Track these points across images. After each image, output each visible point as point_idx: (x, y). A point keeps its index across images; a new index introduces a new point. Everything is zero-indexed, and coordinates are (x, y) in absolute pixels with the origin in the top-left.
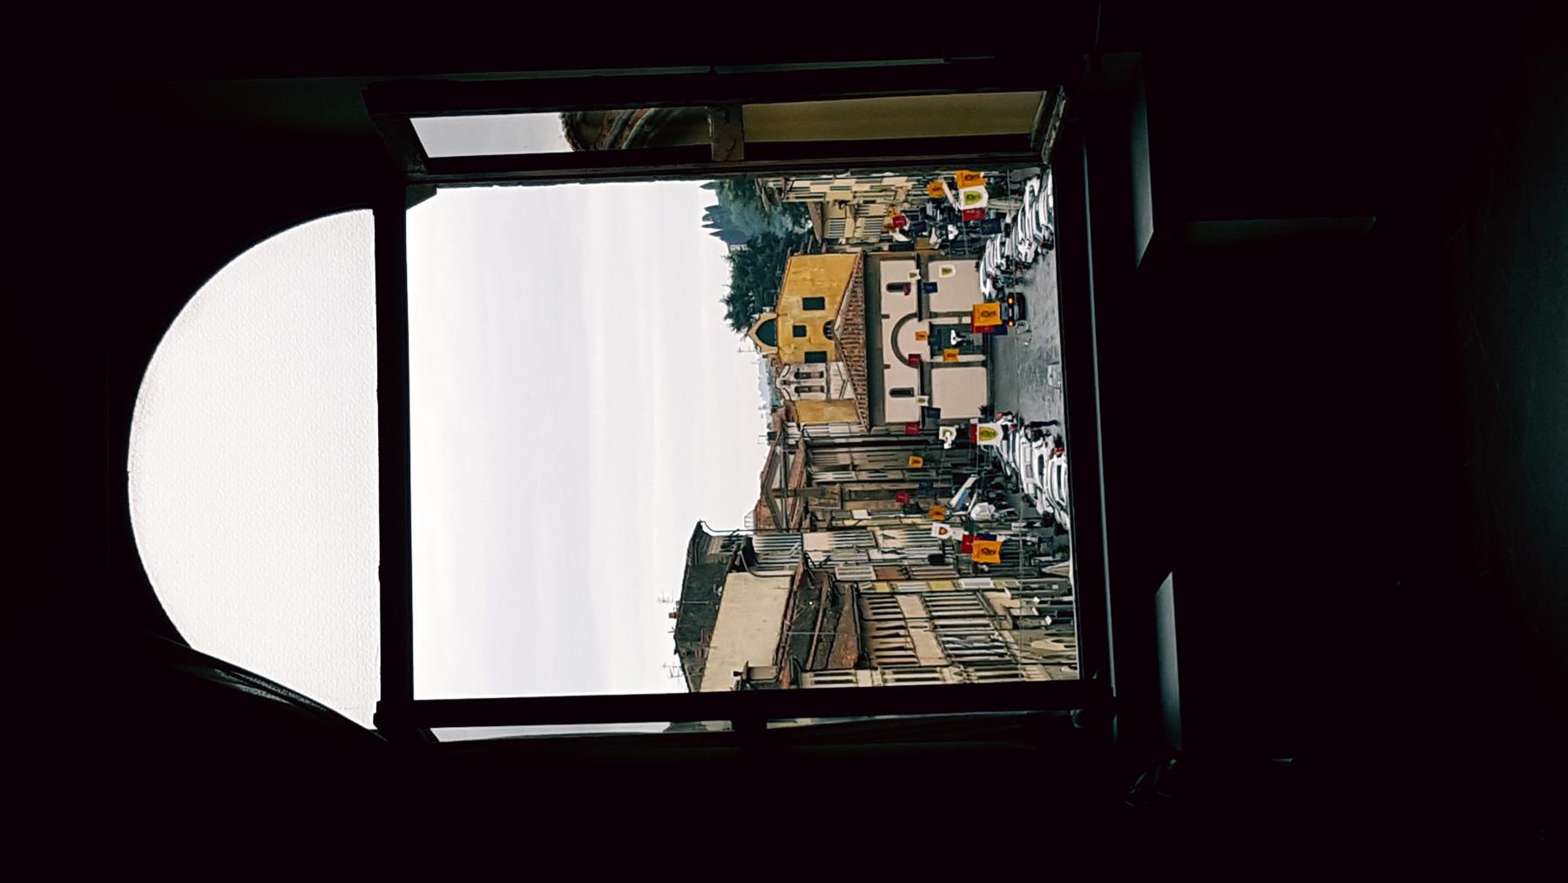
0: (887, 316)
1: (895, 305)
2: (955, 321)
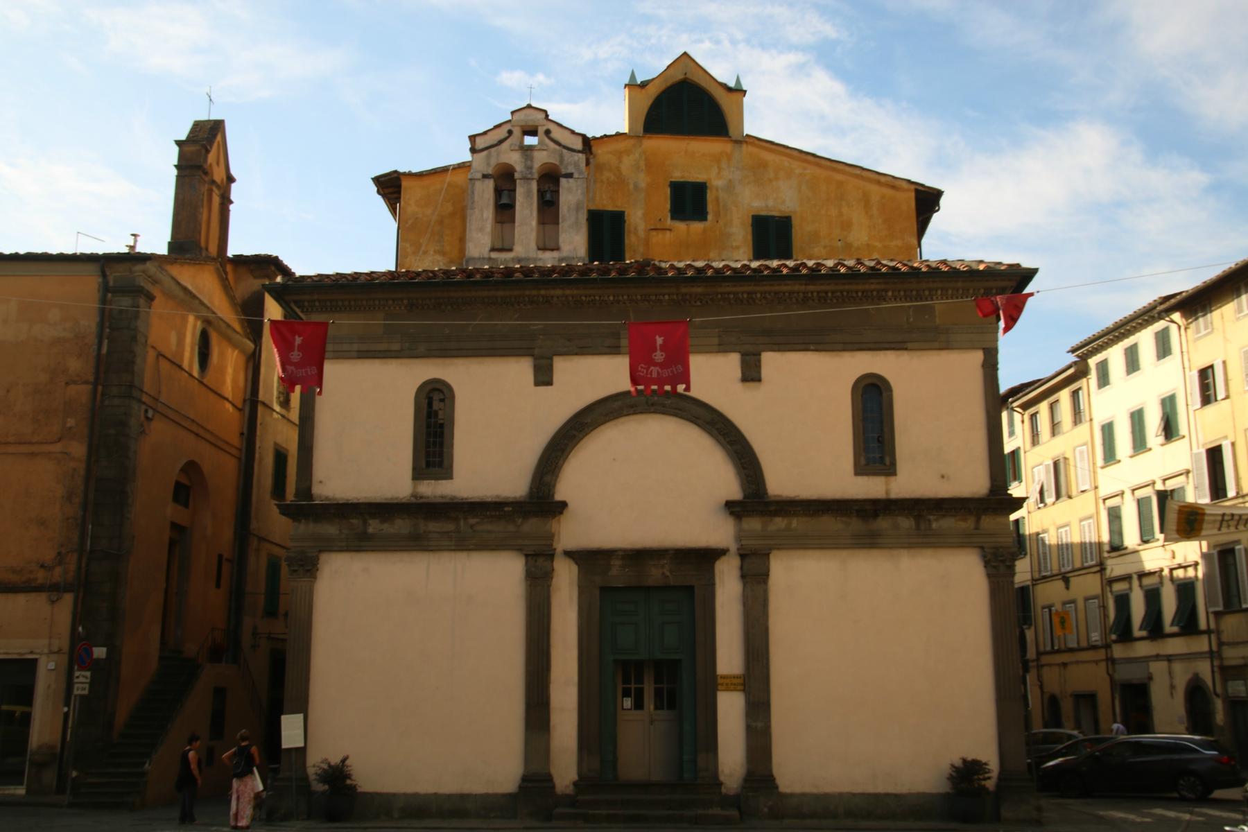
0: (751, 374)
1: (798, 409)
2: (729, 657)
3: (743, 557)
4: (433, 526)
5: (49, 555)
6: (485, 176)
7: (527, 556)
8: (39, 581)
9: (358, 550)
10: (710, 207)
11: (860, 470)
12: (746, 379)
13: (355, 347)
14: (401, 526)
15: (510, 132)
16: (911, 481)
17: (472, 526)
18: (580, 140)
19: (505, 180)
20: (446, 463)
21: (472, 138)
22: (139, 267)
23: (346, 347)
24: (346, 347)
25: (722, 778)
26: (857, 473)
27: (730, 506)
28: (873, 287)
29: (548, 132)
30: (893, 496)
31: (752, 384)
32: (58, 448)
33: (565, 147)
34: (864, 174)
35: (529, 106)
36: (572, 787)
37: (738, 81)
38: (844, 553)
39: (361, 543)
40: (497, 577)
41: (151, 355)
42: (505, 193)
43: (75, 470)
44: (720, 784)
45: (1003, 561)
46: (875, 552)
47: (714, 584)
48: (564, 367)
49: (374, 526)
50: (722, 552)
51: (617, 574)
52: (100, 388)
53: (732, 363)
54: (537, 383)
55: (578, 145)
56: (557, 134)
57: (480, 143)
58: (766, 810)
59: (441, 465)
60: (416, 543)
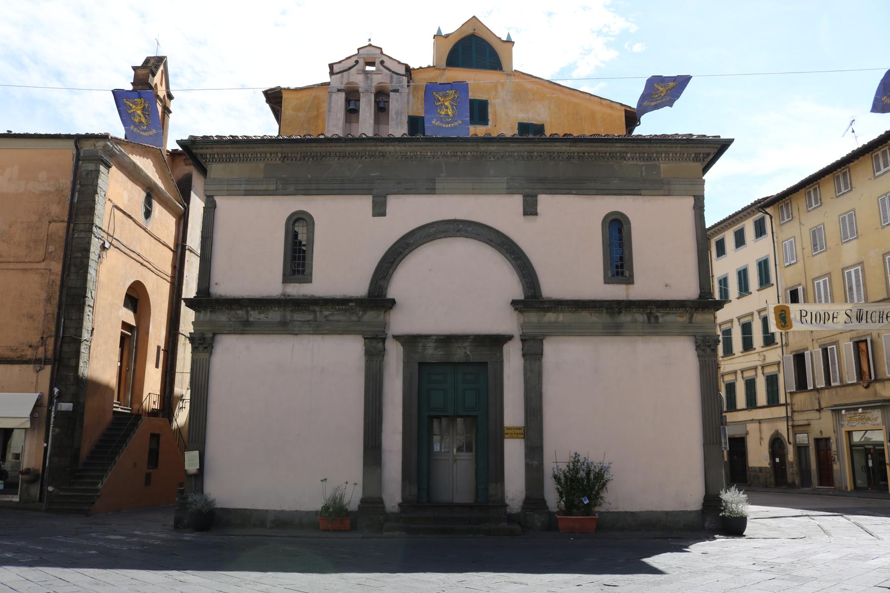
0: (530, 210)
2: (513, 414)
3: (522, 340)
4: (299, 317)
5: (35, 339)
6: (339, 90)
7: (365, 338)
8: (28, 357)
9: (243, 333)
10: (490, 117)
11: (607, 281)
12: (526, 213)
13: (243, 187)
14: (275, 315)
15: (357, 62)
16: (644, 287)
17: (326, 317)
18: (404, 67)
19: (352, 96)
20: (307, 272)
21: (331, 66)
22: (100, 144)
23: (236, 187)
24: (236, 187)
25: (507, 501)
26: (605, 283)
27: (514, 303)
28: (618, 149)
29: (382, 62)
30: (631, 298)
31: (530, 217)
32: (42, 265)
33: (394, 72)
34: (592, 98)
35: (370, 45)
36: (397, 507)
37: (509, 36)
38: (596, 339)
39: (245, 328)
40: (345, 353)
41: (109, 205)
42: (352, 103)
43: (53, 281)
44: (507, 505)
45: (709, 346)
46: (619, 338)
47: (502, 361)
48: (394, 203)
49: (254, 315)
50: (507, 338)
51: (432, 353)
52: (72, 225)
53: (516, 202)
54: (374, 215)
55: (402, 71)
56: (388, 63)
57: (336, 69)
58: (539, 524)
59: (303, 271)
60: (284, 328)
